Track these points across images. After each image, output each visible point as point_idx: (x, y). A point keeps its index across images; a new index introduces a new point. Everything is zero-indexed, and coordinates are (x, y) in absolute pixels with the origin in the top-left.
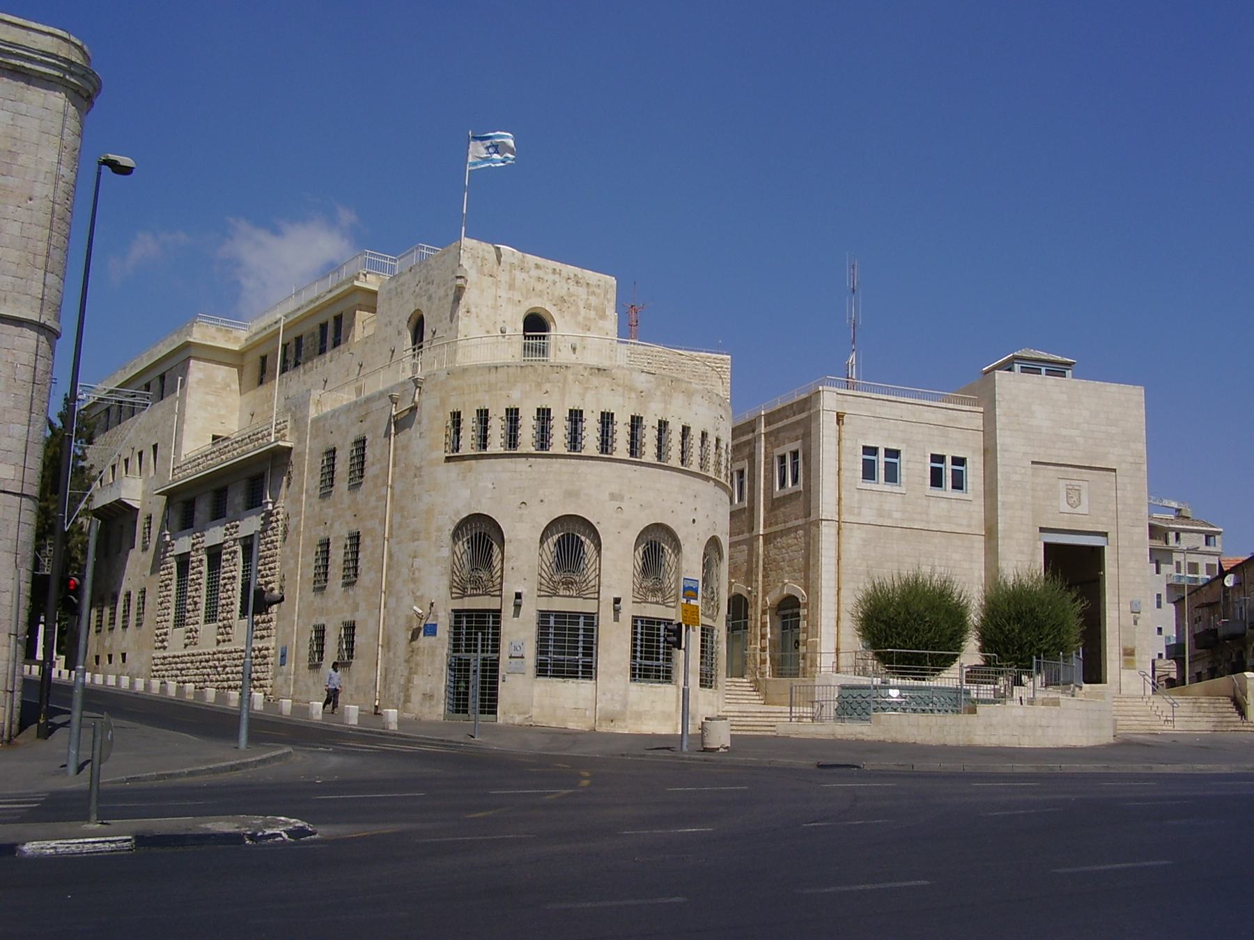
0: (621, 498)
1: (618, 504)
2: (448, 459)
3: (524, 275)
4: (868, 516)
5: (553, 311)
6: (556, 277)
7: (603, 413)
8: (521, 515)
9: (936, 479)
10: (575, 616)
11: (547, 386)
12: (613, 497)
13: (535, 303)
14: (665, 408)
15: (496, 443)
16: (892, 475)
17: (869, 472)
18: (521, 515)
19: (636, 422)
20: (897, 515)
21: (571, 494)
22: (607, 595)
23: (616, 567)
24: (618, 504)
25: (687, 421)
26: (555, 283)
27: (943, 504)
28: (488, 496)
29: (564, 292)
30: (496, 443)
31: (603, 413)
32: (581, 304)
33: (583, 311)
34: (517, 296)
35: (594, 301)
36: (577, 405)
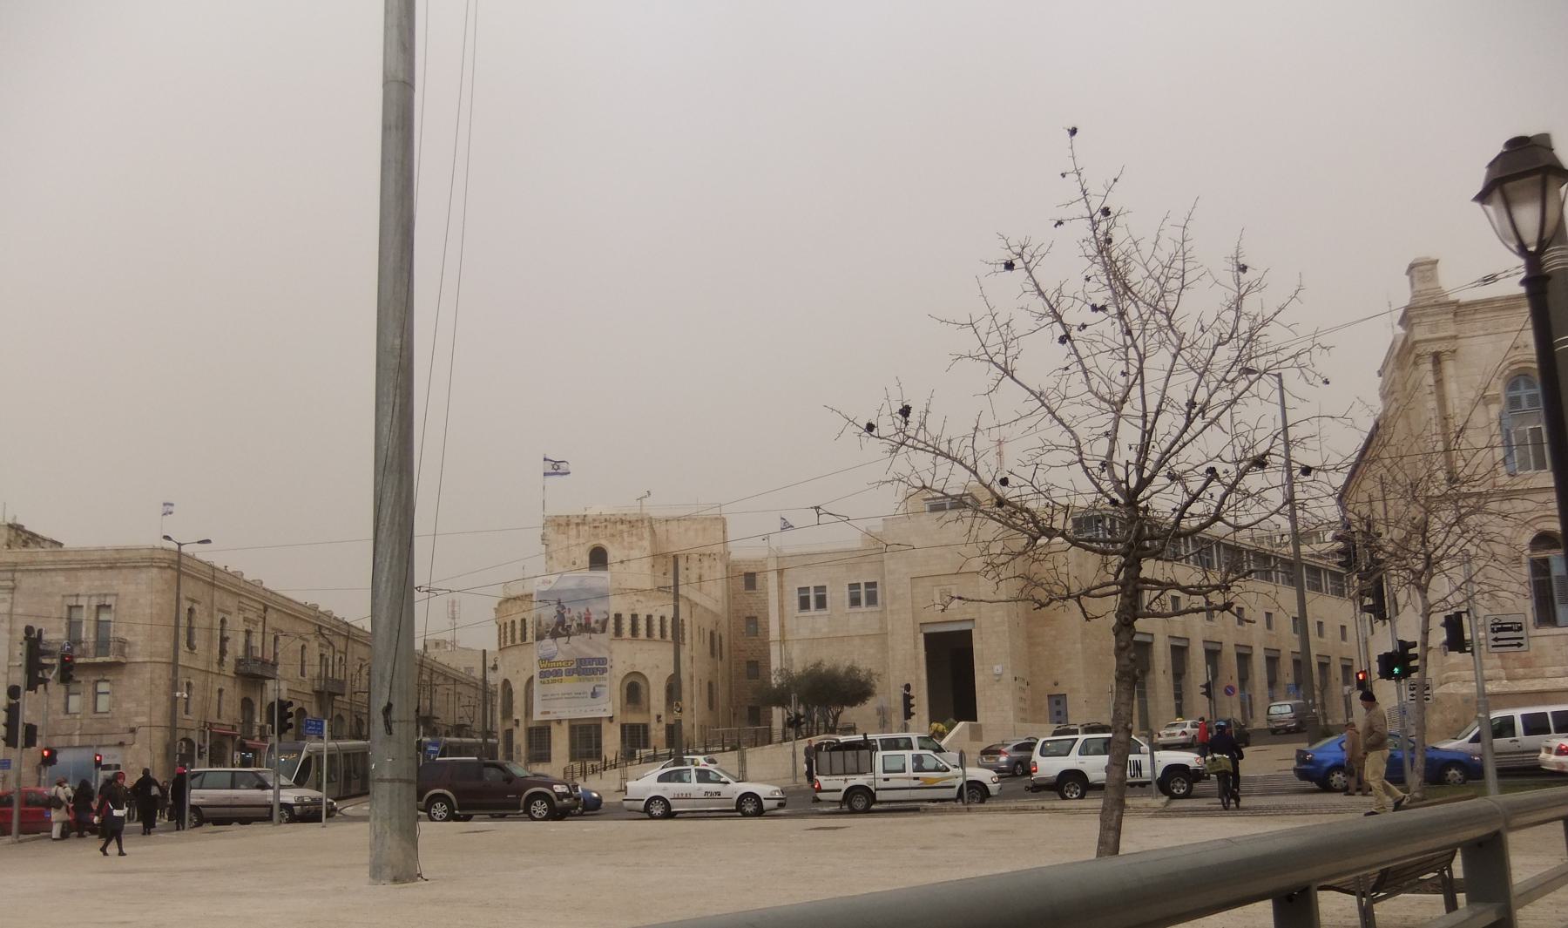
9: (855, 601)
13: (595, 542)
16: (821, 603)
17: (804, 604)
20: (825, 630)
34: (582, 540)
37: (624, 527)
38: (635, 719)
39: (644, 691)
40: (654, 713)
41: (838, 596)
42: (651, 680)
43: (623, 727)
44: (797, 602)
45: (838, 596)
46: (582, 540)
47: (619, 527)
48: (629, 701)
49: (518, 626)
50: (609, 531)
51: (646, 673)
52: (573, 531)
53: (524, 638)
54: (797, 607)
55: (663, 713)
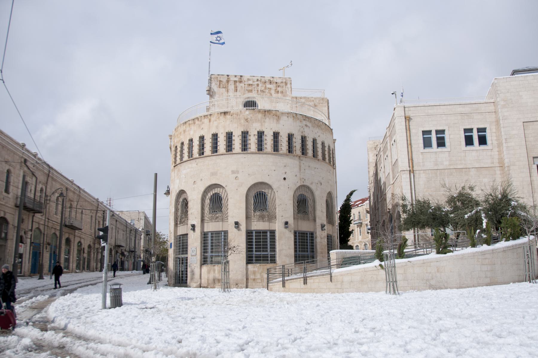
0: (238, 172)
1: (235, 175)
2: (174, 166)
3: (242, 85)
4: (429, 165)
5: (250, 95)
6: (259, 82)
7: (227, 133)
8: (194, 188)
9: (469, 141)
10: (218, 233)
11: (202, 126)
12: (233, 172)
14: (262, 125)
15: (186, 157)
16: (441, 143)
17: (427, 143)
18: (194, 188)
19: (245, 135)
20: (446, 163)
21: (213, 174)
22: (231, 221)
23: (236, 207)
24: (235, 175)
25: (276, 130)
26: (258, 85)
27: (474, 154)
28: (184, 181)
29: (263, 88)
30: (186, 157)
31: (227, 133)
32: (273, 92)
33: (274, 95)
35: (279, 89)
36: (214, 131)
37: (273, 86)
38: (305, 226)
39: (310, 202)
40: (319, 222)
41: (455, 138)
42: (317, 193)
43: (295, 233)
44: (421, 141)
45: (455, 138)
46: (238, 93)
47: (269, 86)
48: (299, 211)
49: (196, 143)
50: (259, 88)
51: (313, 187)
52: (231, 87)
53: (201, 152)
54: (422, 145)
55: (325, 223)
